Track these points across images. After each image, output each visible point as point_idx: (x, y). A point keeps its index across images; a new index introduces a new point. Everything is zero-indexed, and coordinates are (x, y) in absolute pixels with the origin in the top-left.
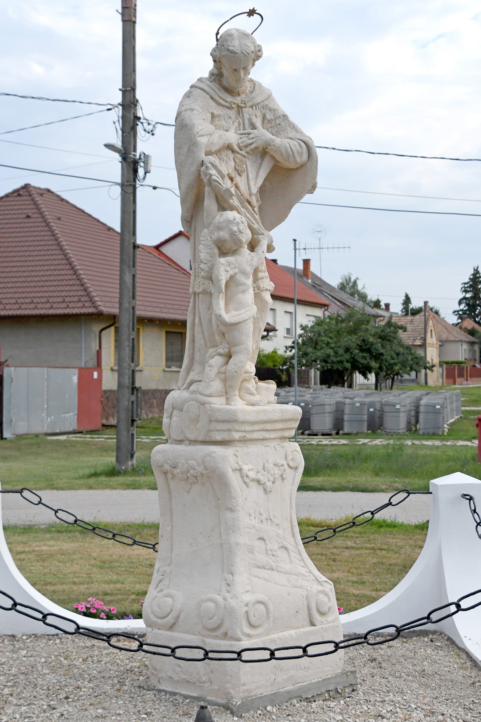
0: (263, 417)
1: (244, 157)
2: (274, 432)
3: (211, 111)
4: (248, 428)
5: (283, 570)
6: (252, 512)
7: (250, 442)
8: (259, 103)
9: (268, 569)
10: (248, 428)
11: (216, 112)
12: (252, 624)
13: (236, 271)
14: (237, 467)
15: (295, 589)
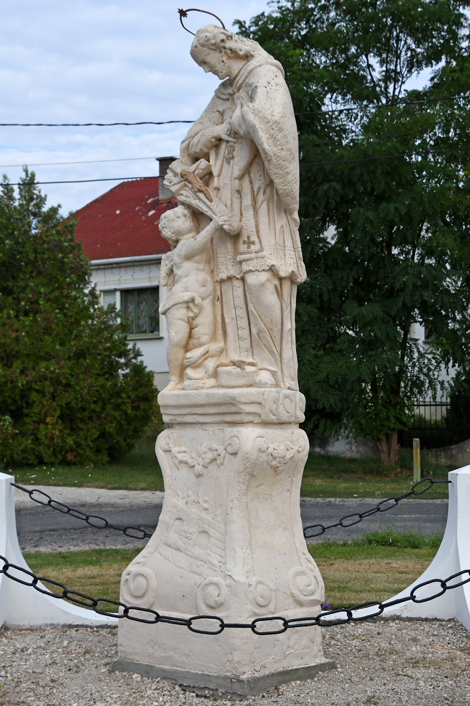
0: (183, 401)
1: (235, 143)
2: (211, 417)
3: (216, 110)
4: (174, 412)
5: (190, 553)
6: (179, 492)
7: (189, 426)
8: (242, 84)
9: (175, 549)
10: (174, 412)
11: (221, 109)
12: (140, 595)
13: (172, 263)
14: (167, 447)
15: (191, 574)
